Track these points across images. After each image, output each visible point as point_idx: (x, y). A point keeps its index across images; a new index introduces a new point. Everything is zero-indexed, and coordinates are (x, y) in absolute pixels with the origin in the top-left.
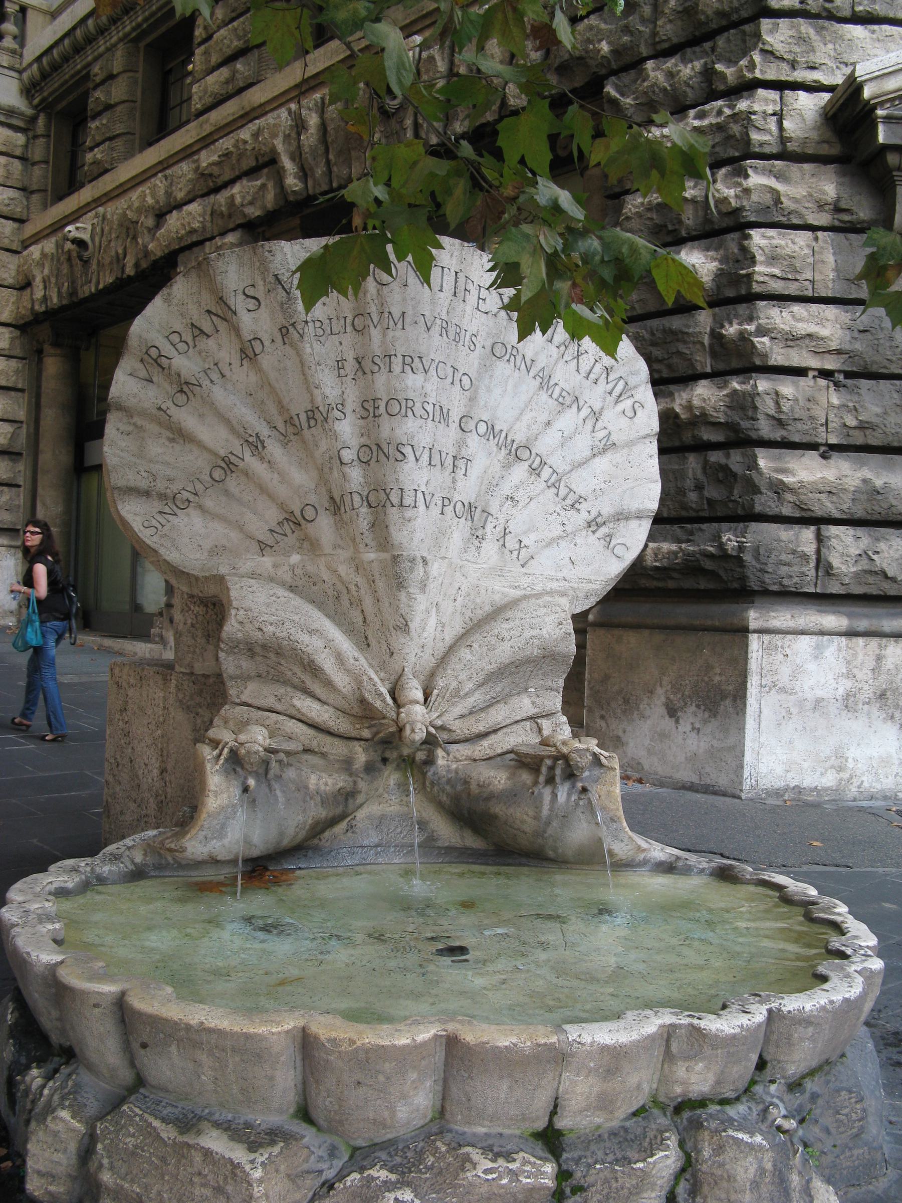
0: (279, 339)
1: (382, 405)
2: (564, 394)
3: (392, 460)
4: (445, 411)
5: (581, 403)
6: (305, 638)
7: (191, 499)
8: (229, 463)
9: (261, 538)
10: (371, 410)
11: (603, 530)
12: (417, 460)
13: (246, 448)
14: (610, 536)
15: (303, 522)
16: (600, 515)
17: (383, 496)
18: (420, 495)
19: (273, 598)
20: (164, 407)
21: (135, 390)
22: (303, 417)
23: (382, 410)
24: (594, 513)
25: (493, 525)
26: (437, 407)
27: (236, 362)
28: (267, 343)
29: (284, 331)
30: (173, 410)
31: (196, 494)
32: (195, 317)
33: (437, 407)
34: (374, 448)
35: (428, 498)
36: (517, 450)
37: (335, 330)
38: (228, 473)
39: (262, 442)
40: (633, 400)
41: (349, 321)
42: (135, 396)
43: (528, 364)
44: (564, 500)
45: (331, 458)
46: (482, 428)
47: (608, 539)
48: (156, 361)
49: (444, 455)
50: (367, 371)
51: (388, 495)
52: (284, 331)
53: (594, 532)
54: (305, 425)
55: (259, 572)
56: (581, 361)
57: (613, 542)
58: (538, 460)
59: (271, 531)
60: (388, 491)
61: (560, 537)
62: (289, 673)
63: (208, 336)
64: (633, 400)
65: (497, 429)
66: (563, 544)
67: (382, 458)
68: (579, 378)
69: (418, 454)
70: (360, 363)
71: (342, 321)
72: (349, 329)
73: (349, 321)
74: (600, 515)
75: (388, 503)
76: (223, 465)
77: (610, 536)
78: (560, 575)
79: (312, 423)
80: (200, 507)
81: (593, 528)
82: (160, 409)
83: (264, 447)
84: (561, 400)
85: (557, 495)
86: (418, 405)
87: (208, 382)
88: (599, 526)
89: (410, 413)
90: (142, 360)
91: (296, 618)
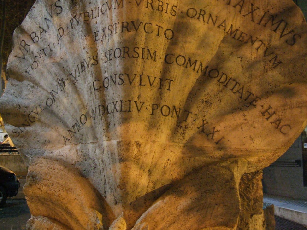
0: (70, 27)
1: (112, 52)
2: (243, 35)
3: (117, 83)
4: (152, 52)
5: (254, 39)
6: (63, 194)
7: (36, 116)
8: (53, 96)
9: (65, 135)
10: (108, 56)
11: (274, 117)
12: (131, 83)
13: (59, 87)
14: (279, 120)
15: (81, 125)
16: (270, 107)
17: (113, 106)
18: (133, 104)
19: (51, 170)
20: (28, 71)
21: (17, 64)
22: (80, 66)
23: (112, 55)
24: (266, 107)
25: (193, 119)
26: (146, 50)
27: (56, 42)
28: (65, 30)
29: (72, 21)
30: (32, 72)
31: (37, 114)
32: (41, 23)
33: (146, 50)
34: (110, 78)
35: (139, 105)
36: (209, 72)
37: (94, 16)
38: (53, 101)
39: (64, 83)
40: (293, 33)
41: (100, 9)
42: (17, 66)
43: (214, 19)
44: (245, 100)
45: (91, 87)
46: (181, 61)
47: (278, 123)
48: (24, 47)
49: (152, 79)
50: (107, 35)
51: (115, 105)
52: (72, 21)
53: (267, 119)
54: (81, 70)
55: (62, 154)
56: (254, 14)
57: (282, 124)
58: (224, 76)
59: (69, 131)
60: (115, 103)
61: (242, 124)
62: (60, 215)
63: (46, 32)
64: (293, 33)
65: (193, 60)
66: (245, 128)
67: (113, 84)
68: (253, 24)
69: (131, 79)
70: (104, 31)
71: (97, 10)
72: (100, 13)
73: (100, 9)
74: (270, 107)
75: (115, 111)
76: (52, 97)
77: (279, 120)
78: (243, 147)
79: (83, 69)
80: (40, 121)
81: (267, 115)
82: (26, 72)
83: (65, 85)
84: (241, 39)
85: (241, 97)
86: (131, 49)
87: (43, 55)
88: (271, 115)
89: (126, 55)
90: (20, 49)
91: (61, 182)
